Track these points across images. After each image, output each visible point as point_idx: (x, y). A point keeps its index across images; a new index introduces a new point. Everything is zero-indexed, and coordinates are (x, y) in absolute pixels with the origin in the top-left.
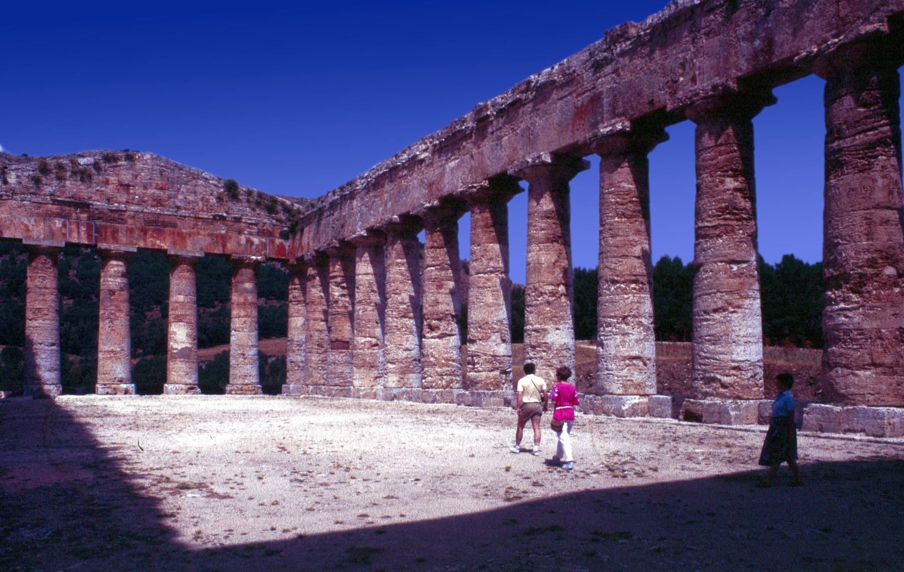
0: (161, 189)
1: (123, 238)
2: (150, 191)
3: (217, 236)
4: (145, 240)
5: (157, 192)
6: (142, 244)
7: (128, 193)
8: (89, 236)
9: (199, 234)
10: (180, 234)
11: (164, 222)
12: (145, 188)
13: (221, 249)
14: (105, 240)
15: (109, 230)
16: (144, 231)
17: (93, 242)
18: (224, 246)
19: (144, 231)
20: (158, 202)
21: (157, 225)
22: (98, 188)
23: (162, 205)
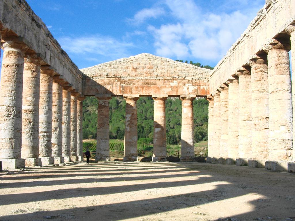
0: (150, 68)
1: (134, 92)
2: (145, 70)
3: (174, 87)
4: (143, 91)
5: (148, 70)
6: (142, 94)
7: (136, 71)
8: (121, 91)
9: (166, 87)
10: (158, 88)
11: (151, 83)
12: (143, 68)
13: (176, 93)
14: (127, 93)
15: (128, 88)
16: (143, 88)
17: (121, 94)
18: (177, 92)
19: (143, 88)
20: (149, 74)
21: (148, 85)
22: (124, 71)
23: (150, 75)
